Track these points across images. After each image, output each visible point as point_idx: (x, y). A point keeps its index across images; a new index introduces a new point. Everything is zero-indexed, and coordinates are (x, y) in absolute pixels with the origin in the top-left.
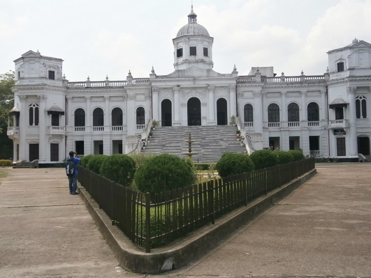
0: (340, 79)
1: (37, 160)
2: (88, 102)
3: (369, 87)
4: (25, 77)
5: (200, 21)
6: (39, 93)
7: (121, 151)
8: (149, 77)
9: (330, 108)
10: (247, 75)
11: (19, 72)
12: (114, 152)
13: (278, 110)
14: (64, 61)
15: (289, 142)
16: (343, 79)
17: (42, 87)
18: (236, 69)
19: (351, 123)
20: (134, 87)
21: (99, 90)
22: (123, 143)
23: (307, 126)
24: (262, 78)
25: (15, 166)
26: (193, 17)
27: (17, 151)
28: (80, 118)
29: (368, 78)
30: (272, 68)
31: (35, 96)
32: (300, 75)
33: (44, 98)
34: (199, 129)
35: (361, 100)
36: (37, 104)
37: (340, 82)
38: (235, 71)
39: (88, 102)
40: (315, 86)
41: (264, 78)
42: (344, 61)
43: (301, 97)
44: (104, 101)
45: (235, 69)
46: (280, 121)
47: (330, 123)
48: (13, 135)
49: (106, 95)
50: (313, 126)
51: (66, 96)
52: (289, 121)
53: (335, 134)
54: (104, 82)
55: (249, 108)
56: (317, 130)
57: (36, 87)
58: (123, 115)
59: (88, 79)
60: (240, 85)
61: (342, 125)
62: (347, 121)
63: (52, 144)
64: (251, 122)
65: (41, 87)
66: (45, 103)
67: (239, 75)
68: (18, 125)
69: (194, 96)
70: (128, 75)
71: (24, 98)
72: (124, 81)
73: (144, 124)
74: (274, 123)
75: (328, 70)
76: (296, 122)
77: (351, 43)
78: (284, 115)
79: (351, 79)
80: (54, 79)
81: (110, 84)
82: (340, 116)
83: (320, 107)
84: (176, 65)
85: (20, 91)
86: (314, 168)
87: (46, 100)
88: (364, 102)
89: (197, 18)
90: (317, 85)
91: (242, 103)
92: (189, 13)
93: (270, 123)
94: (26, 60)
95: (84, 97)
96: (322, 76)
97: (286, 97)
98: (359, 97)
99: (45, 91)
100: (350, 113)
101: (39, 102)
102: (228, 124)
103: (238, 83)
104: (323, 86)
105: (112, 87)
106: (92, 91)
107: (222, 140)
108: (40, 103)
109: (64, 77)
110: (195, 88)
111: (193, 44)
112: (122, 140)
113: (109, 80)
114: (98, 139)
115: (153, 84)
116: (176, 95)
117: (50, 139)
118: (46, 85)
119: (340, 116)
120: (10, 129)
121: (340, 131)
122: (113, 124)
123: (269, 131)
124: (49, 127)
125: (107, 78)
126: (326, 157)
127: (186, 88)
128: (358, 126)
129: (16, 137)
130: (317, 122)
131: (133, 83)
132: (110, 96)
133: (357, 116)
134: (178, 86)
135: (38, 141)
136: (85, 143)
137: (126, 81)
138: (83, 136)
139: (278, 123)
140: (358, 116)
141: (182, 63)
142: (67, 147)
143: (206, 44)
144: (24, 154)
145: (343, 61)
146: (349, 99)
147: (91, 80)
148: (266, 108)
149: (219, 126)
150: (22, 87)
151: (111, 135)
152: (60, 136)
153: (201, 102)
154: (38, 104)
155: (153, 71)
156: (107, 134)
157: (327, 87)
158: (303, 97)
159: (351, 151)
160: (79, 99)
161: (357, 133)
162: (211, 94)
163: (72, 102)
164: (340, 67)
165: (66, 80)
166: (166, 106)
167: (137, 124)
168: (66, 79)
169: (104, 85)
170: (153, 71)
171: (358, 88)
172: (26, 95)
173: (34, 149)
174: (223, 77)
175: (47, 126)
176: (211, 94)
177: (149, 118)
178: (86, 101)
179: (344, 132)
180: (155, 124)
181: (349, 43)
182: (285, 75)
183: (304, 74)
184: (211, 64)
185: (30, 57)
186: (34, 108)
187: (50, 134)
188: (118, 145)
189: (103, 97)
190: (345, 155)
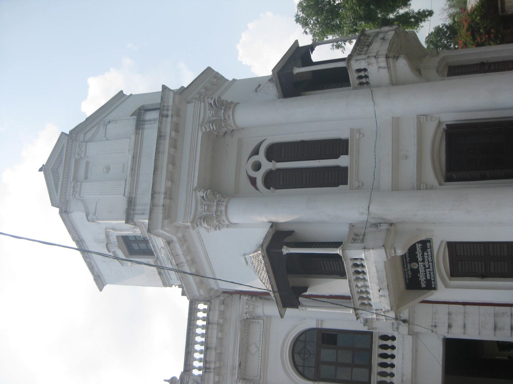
0: (175, 255)
3: (207, 135)
19: (364, 218)
29: (167, 143)
35: (267, 166)
40: (220, 340)
42: (114, 235)
50: (394, 361)
53: (430, 286)
56: (415, 351)
79: (159, 212)
83: (312, 324)
88: (276, 151)
90: (215, 331)
98: (253, 174)
104: (222, 308)
121: (415, 266)
128: (386, 178)
130: (377, 342)
133: (336, 184)
140: (337, 178)
161: (420, 186)
179: (419, 246)
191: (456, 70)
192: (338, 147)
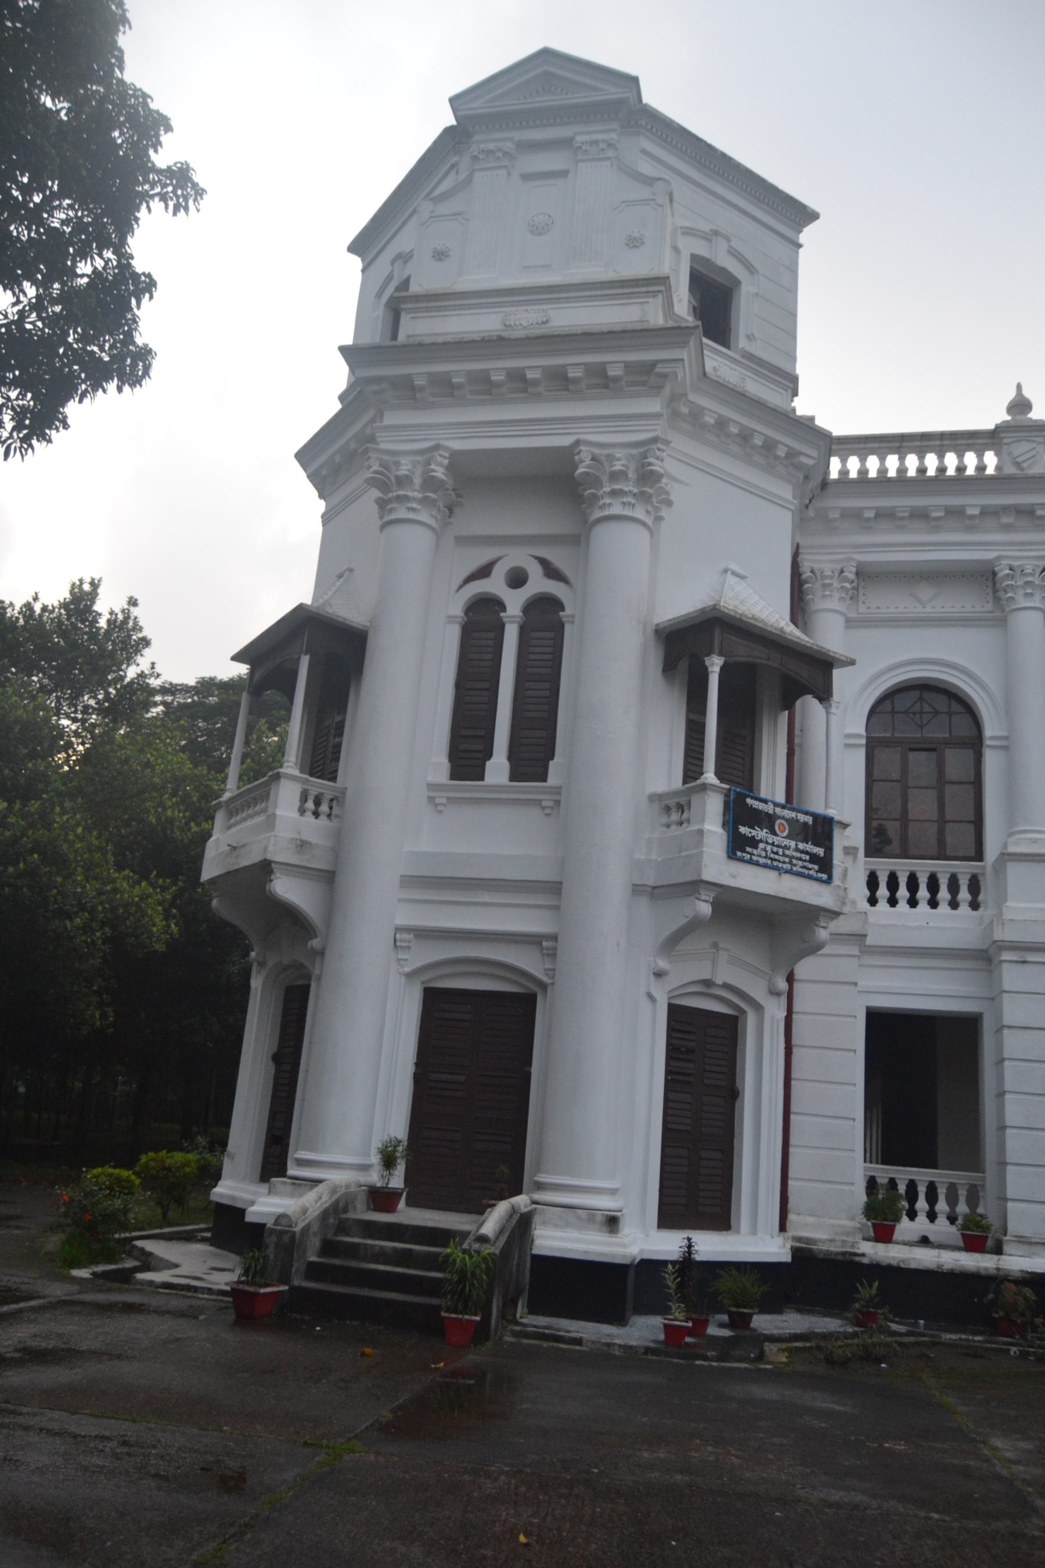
1: (521, 1201)
4: (459, 287)
6: (593, 428)
14: (812, 216)
27: (277, 1058)
36: (544, 563)
48: (265, 868)
51: (796, 555)
59: (1020, 405)
63: (680, 1019)
65: (627, 365)
66: (645, 533)
71: (430, 483)
80: (728, 347)
87: (659, 519)
94: (491, 146)
117: (671, 944)
135: (528, 961)
136: (1013, 1044)
154: (557, 557)
160: (925, 592)
163: (850, 623)
172: (457, 462)
173: (481, 1056)
175: (654, 798)
186: (514, 602)
187: (695, 886)
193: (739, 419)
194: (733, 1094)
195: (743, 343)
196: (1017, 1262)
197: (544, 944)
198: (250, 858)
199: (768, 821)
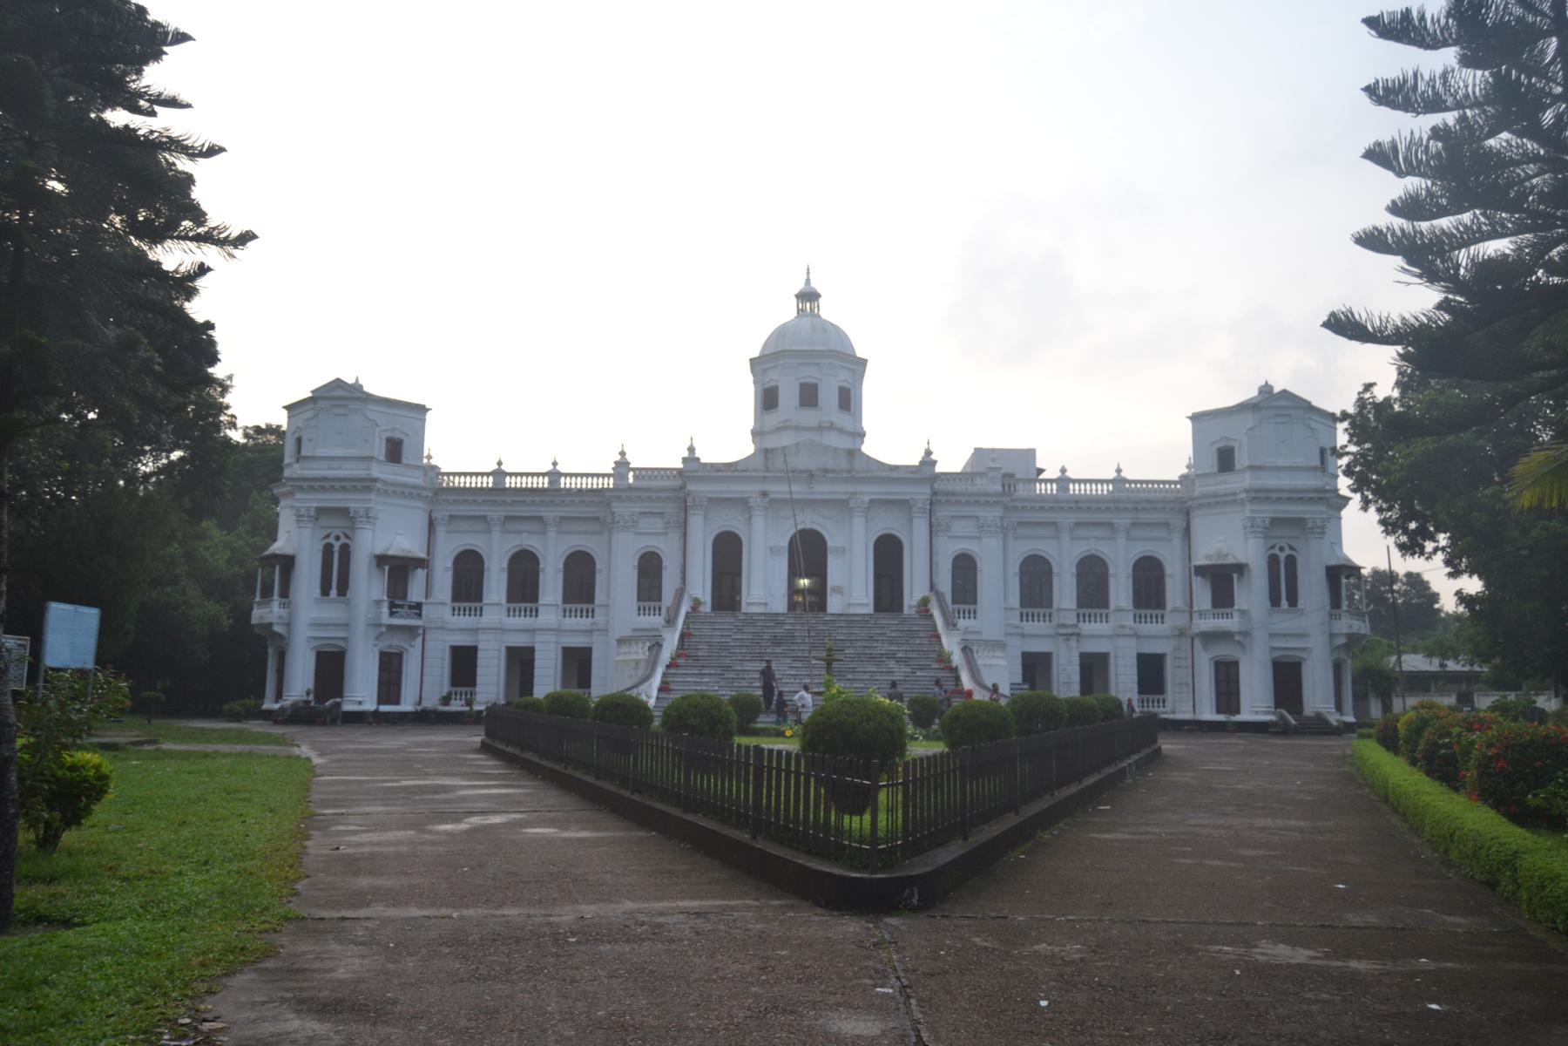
2: (496, 534)
5: (828, 310)
6: (352, 502)
7: (585, 680)
8: (681, 466)
9: (1197, 574)
10: (958, 469)
11: (299, 440)
12: (565, 684)
13: (1049, 573)
15: (1077, 668)
16: (1235, 494)
17: (366, 485)
18: (928, 453)
20: (634, 494)
21: (529, 499)
22: (595, 656)
23: (1130, 623)
24: (1003, 481)
25: (269, 716)
26: (808, 296)
28: (468, 580)
30: (1030, 454)
31: (344, 512)
32: (1112, 475)
33: (368, 516)
34: (826, 622)
35: (1282, 556)
37: (1226, 503)
38: (928, 461)
39: (496, 534)
41: (1009, 479)
43: (1113, 539)
44: (544, 533)
45: (928, 453)
46: (1055, 605)
47: (1195, 616)
48: (271, 624)
49: (549, 513)
52: (1080, 605)
54: (544, 475)
55: (965, 567)
57: (348, 485)
58: (598, 576)
59: (500, 463)
60: (943, 499)
61: (1230, 623)
62: (1243, 612)
63: (382, 654)
64: (972, 607)
67: (939, 469)
68: (285, 593)
69: (808, 526)
70: (618, 458)
72: (603, 476)
73: (660, 599)
74: (1036, 611)
75: (1188, 467)
76: (1098, 611)
77: (1255, 393)
78: (1065, 592)
81: (565, 483)
82: (1223, 598)
83: (1168, 571)
84: (756, 434)
85: (298, 496)
86: (1155, 741)
88: (1291, 561)
89: (821, 300)
91: (948, 550)
92: (799, 286)
93: (1025, 611)
95: (483, 518)
96: (1175, 483)
97: (1072, 538)
99: (372, 496)
100: (1251, 595)
101: (353, 528)
102: (906, 610)
103: (935, 493)
105: (569, 491)
106: (509, 499)
107: (891, 656)
108: (358, 532)
109: (429, 457)
110: (814, 501)
111: (810, 374)
112: (590, 649)
113: (561, 468)
114: (519, 641)
115: (690, 487)
116: (759, 522)
117: (378, 637)
118: (376, 480)
119: (1223, 598)
120: (259, 604)
122: (567, 598)
123: (1023, 635)
124: (378, 603)
125: (555, 464)
126: (1188, 716)
127: (784, 501)
129: (277, 629)
130: (1159, 612)
131: (631, 480)
132: (562, 518)
134: (764, 494)
135: (341, 643)
136: (480, 654)
137: (609, 476)
138: (476, 630)
139: (1047, 611)
140: (1275, 601)
141: (778, 430)
142: (427, 662)
143: (843, 378)
144: (300, 681)
145: (1231, 443)
146: (1248, 550)
147: (506, 468)
148: (1014, 568)
149: (882, 615)
150: (304, 484)
151: (558, 631)
152: (411, 631)
153: (830, 544)
154: (348, 532)
155: (691, 449)
156: (550, 627)
157: (1188, 514)
158: (1121, 540)
159: (1256, 703)
162: (859, 522)
164: (1226, 459)
165: (435, 468)
166: (728, 553)
167: (639, 599)
168: (433, 462)
169: (544, 483)
170: (691, 449)
171: (1274, 521)
174: (894, 475)
176: (859, 522)
177: (678, 585)
178: (489, 531)
180: (697, 604)
181: (1251, 393)
182: (1070, 474)
183: (1123, 474)
184: (861, 435)
185: (338, 399)
186: (337, 546)
187: (381, 625)
188: (578, 662)
189: (540, 519)
190: (1238, 712)
191: (1338, 668)
192: (1293, 600)
193: (399, 490)
194: (400, 673)
195: (405, 461)
196: (476, 708)
197: (345, 639)
198: (266, 621)
199: (402, 606)
